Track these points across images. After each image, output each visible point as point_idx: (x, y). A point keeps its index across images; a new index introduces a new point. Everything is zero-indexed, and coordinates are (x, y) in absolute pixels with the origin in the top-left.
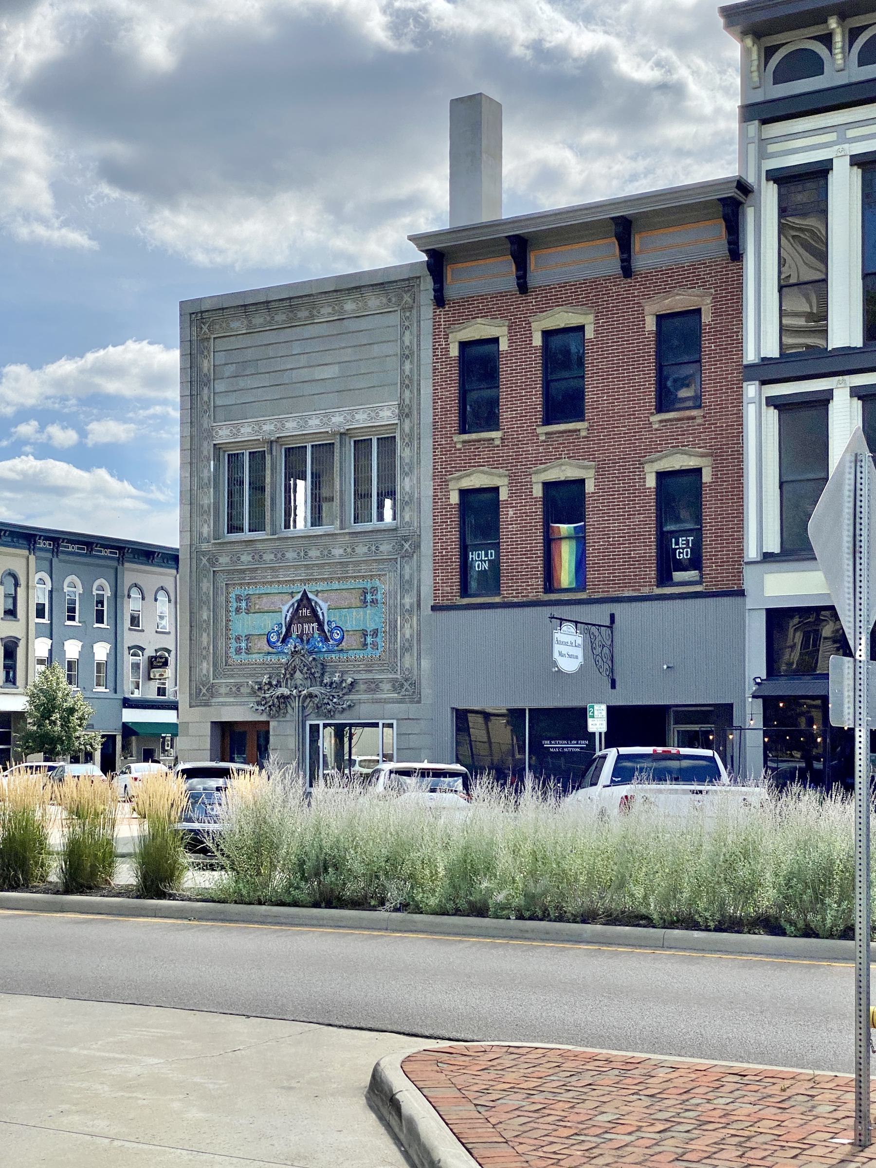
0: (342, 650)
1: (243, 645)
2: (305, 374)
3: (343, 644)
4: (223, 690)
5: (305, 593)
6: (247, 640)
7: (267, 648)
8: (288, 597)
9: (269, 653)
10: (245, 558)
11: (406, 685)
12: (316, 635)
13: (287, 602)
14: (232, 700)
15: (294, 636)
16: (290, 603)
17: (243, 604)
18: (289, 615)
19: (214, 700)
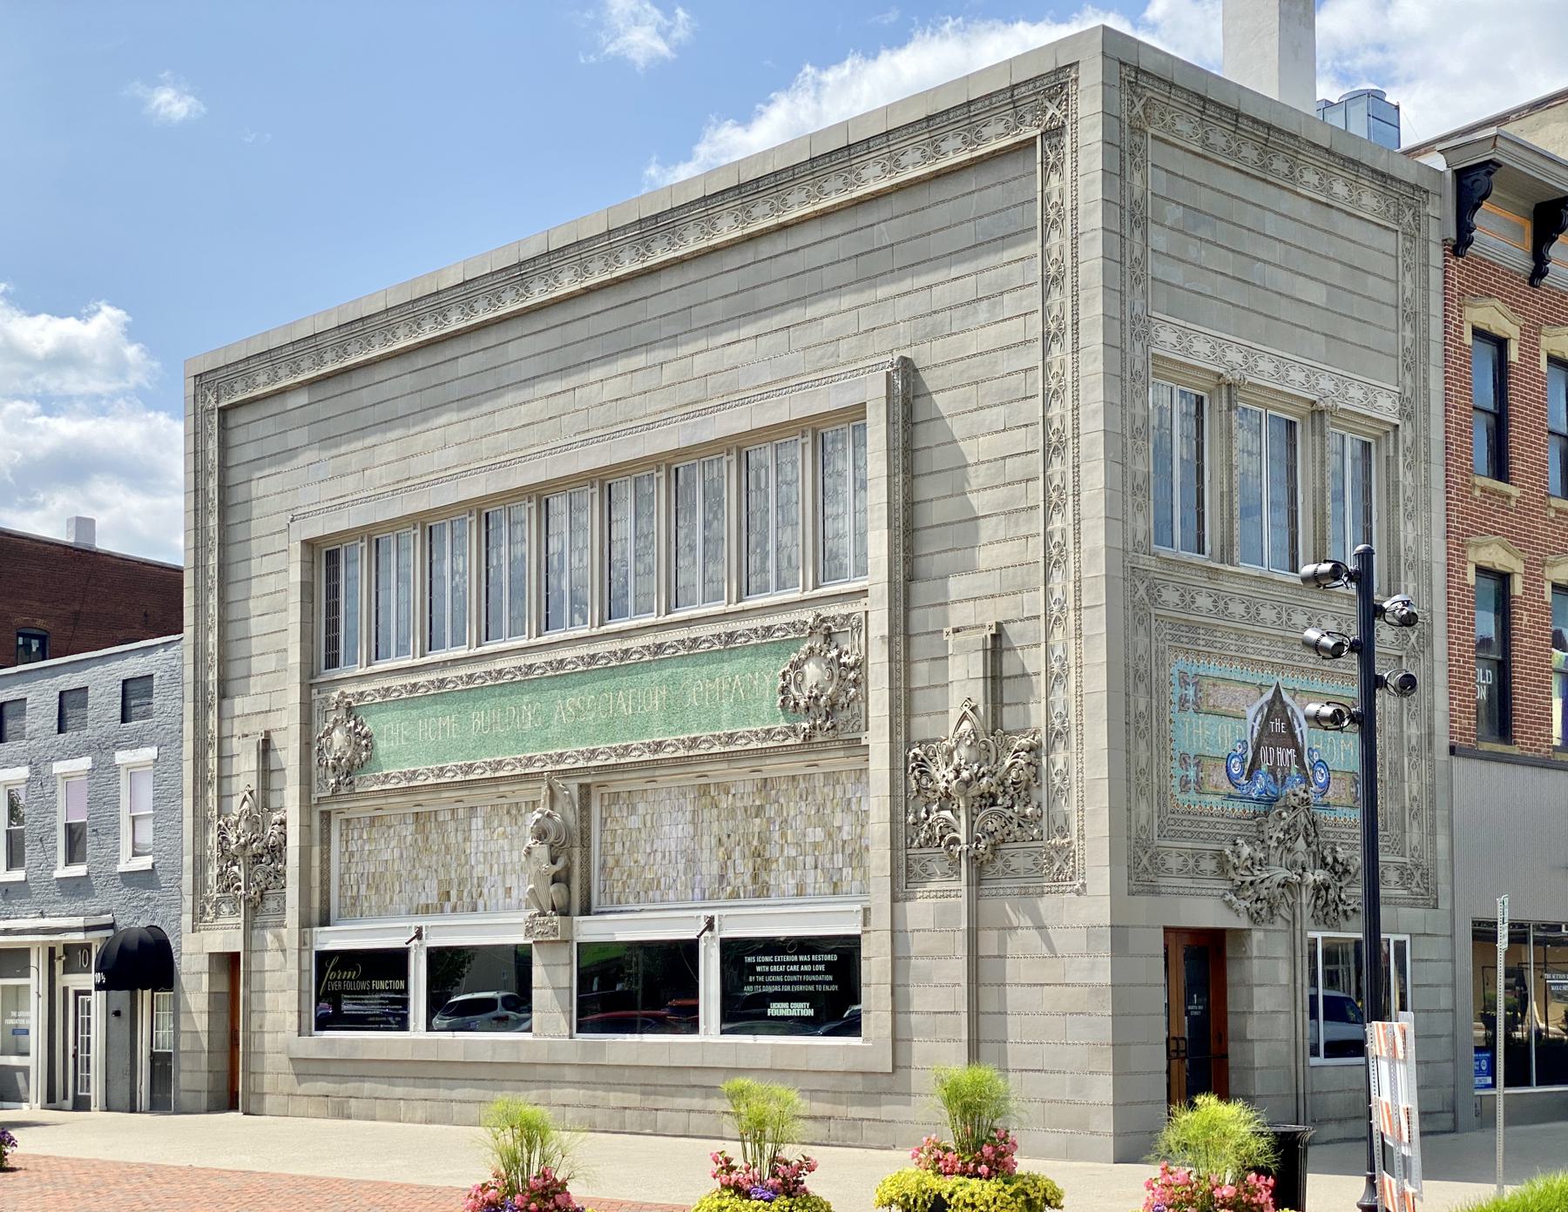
0: (1328, 805)
1: (1192, 774)
2: (1281, 280)
3: (1330, 793)
4: (1173, 863)
5: (1278, 691)
6: (1197, 765)
7: (1226, 787)
8: (1254, 693)
9: (1230, 796)
10: (1204, 602)
11: (1417, 875)
12: (1294, 772)
13: (1254, 701)
14: (1188, 883)
15: (1264, 769)
16: (1258, 705)
17: (1191, 692)
18: (1257, 727)
19: (1163, 881)
